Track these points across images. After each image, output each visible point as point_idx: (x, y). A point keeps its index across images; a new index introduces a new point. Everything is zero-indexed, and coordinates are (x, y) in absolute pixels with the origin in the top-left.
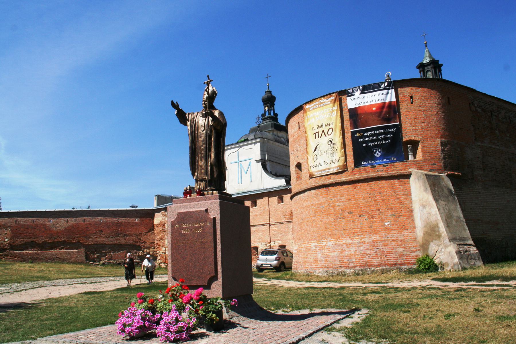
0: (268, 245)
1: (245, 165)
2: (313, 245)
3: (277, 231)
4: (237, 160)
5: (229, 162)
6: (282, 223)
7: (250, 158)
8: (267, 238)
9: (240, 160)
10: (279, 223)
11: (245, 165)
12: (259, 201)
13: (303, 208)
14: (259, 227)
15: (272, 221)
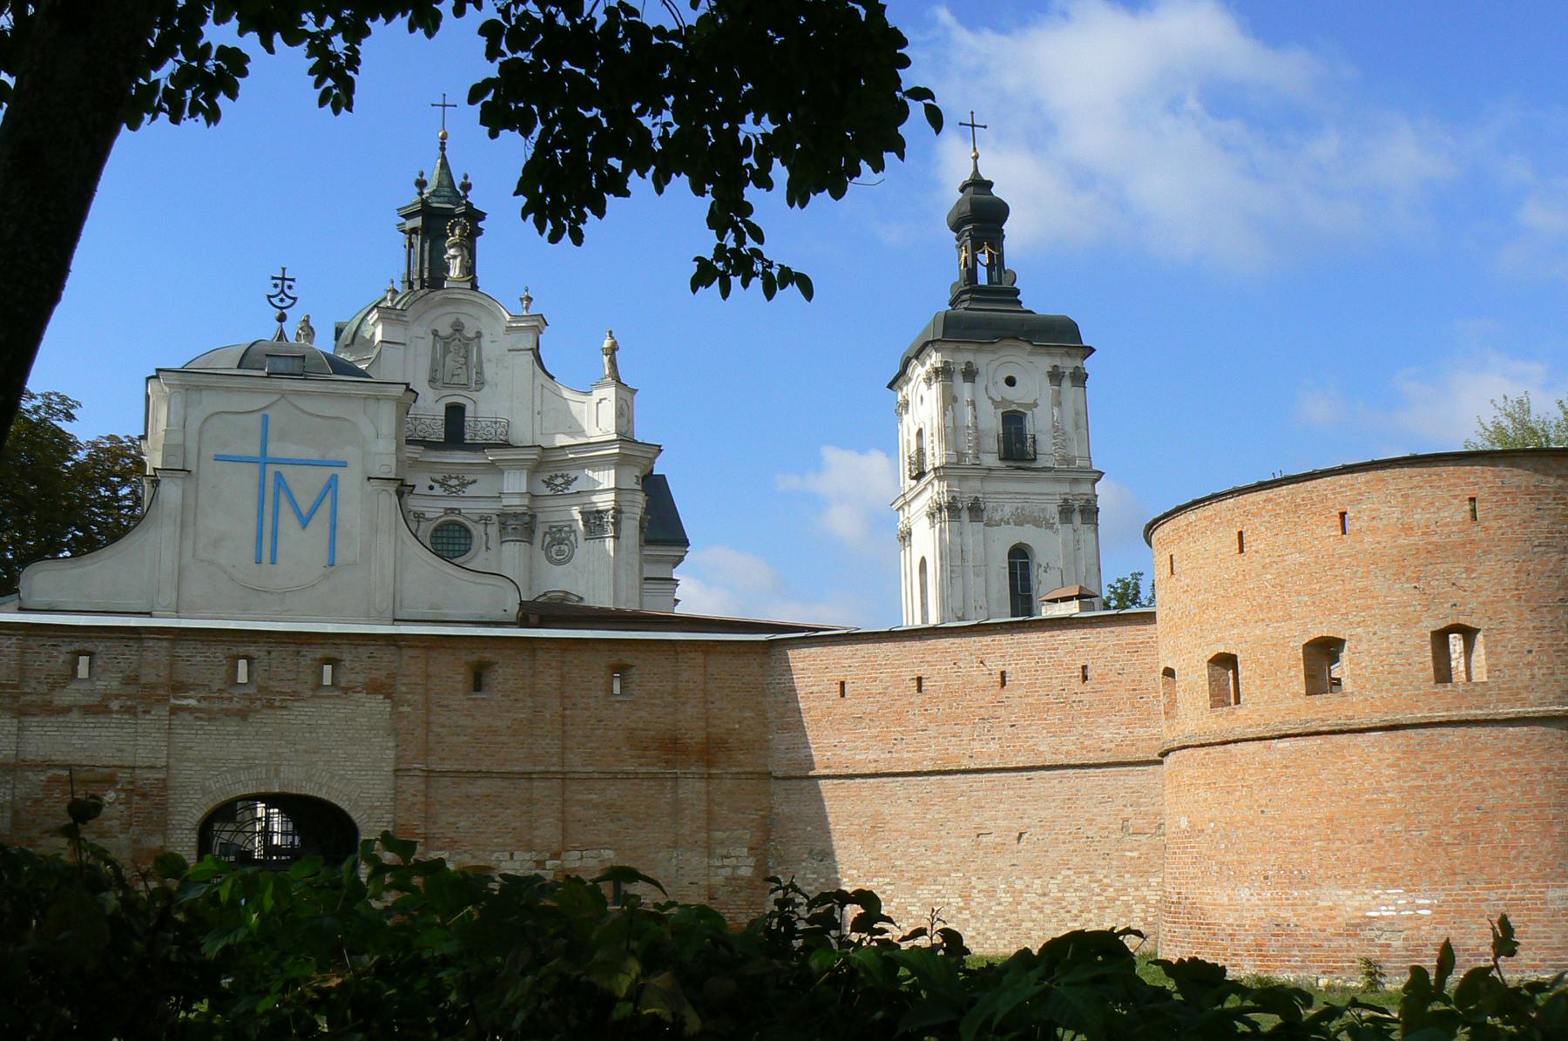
0: (549, 864)
1: (306, 484)
2: (1551, 894)
3: (596, 806)
4: (254, 451)
5: (209, 452)
6: (627, 776)
7: (331, 456)
8: (547, 831)
9: (274, 450)
10: (614, 777)
11: (306, 484)
12: (504, 676)
13: (1492, 773)
14: (505, 783)
15: (576, 762)
